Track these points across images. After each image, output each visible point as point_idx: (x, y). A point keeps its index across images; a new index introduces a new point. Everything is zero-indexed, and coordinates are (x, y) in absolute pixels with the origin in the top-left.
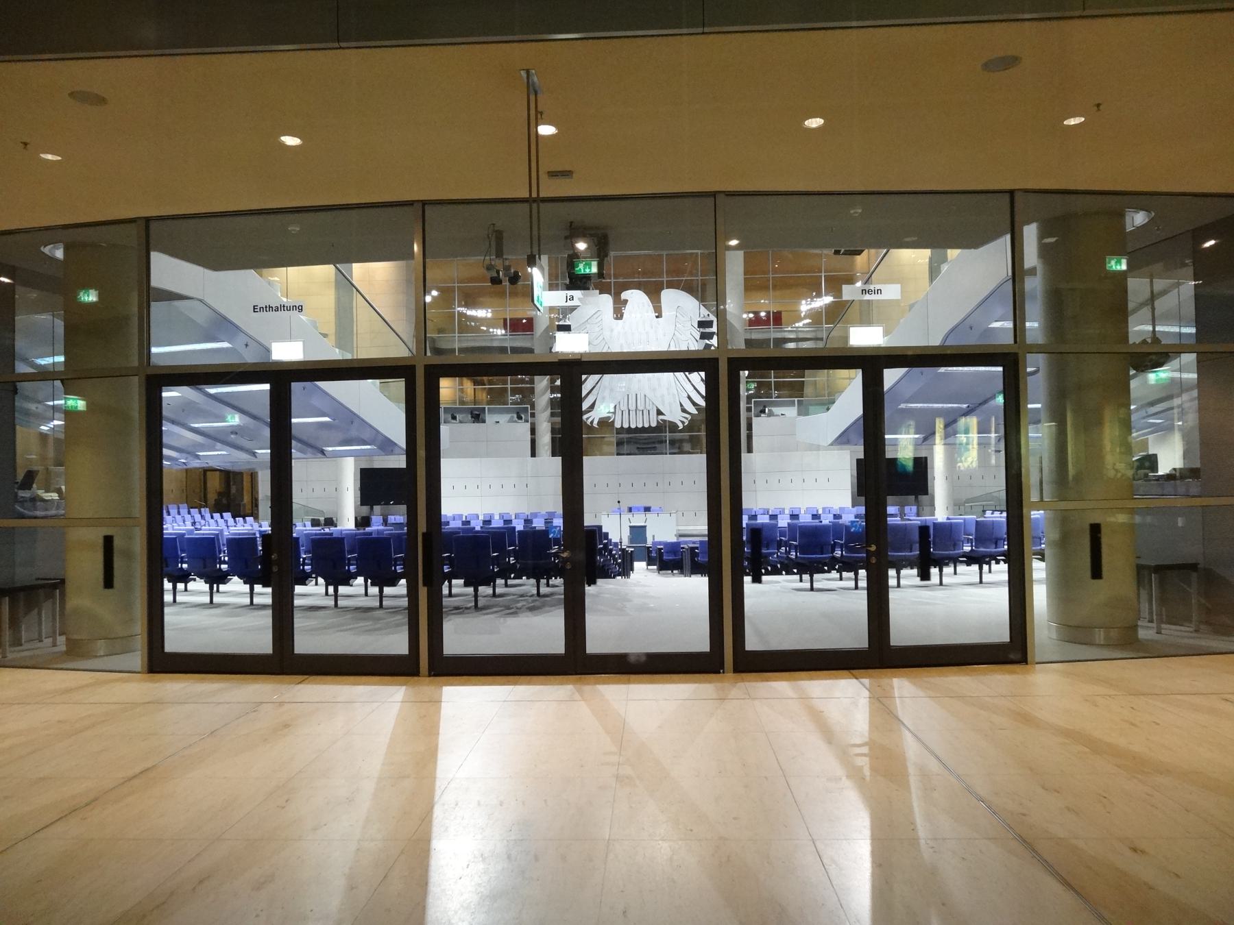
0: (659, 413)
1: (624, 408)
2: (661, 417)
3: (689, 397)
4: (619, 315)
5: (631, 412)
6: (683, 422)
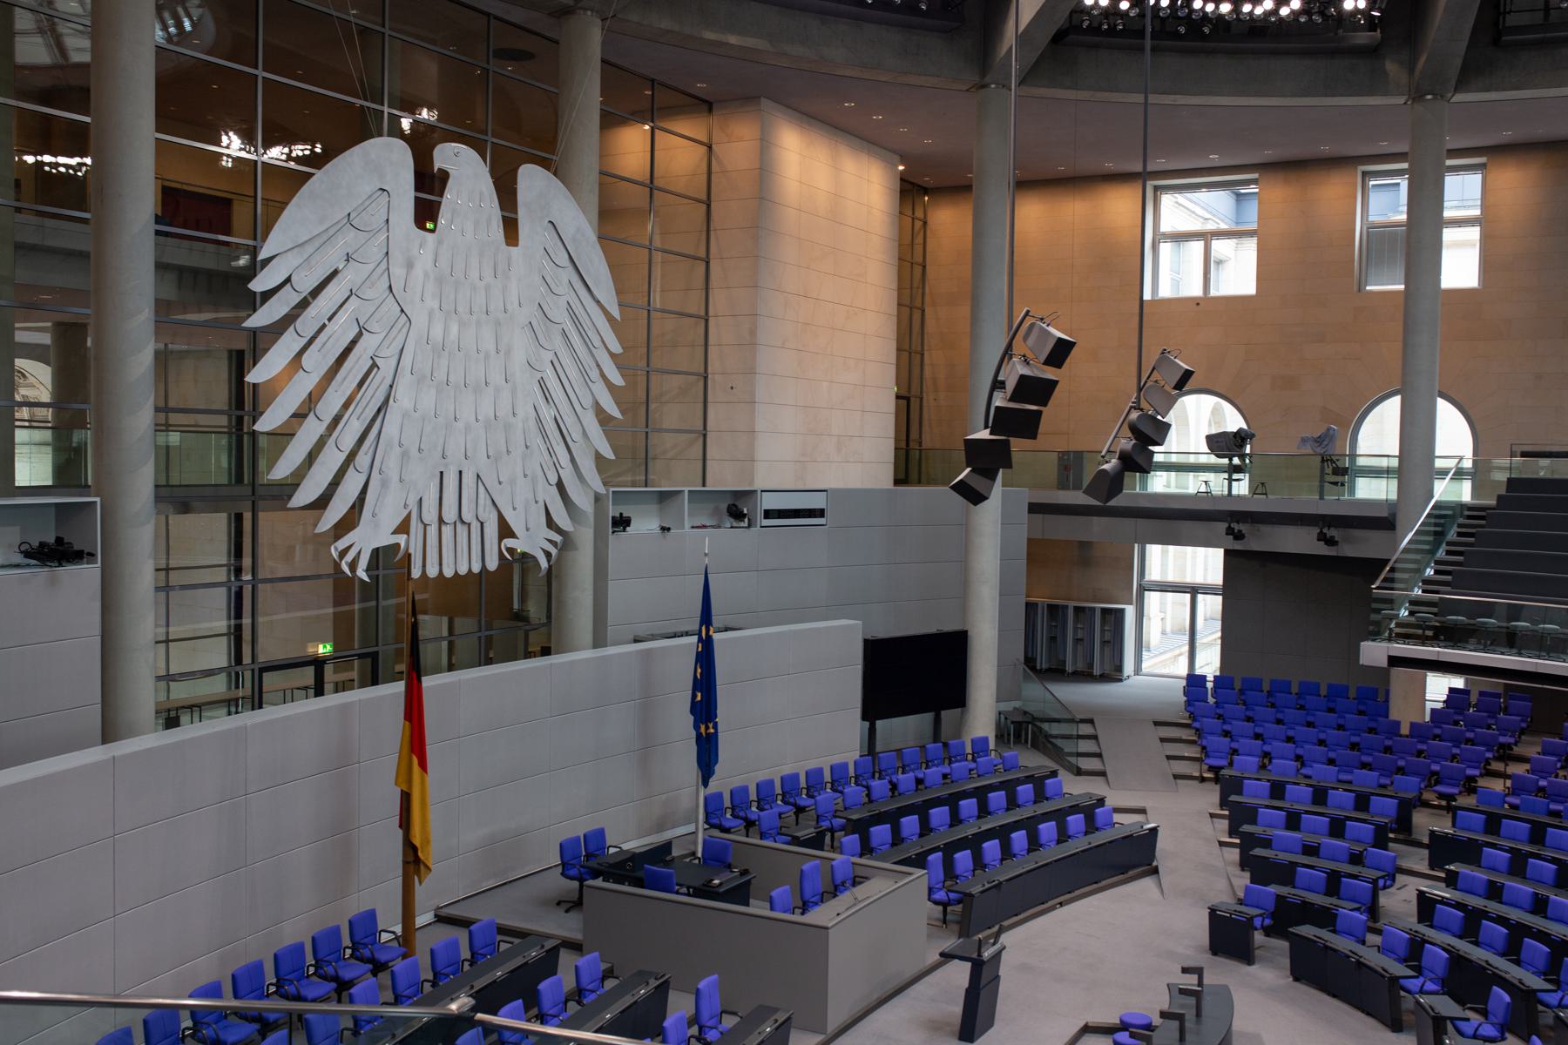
0: (505, 531)
1: (430, 515)
2: (509, 542)
3: (560, 485)
4: (426, 213)
5: (444, 528)
6: (548, 555)
